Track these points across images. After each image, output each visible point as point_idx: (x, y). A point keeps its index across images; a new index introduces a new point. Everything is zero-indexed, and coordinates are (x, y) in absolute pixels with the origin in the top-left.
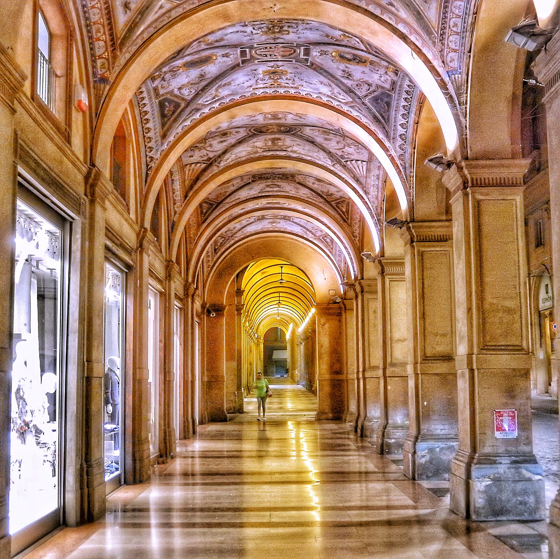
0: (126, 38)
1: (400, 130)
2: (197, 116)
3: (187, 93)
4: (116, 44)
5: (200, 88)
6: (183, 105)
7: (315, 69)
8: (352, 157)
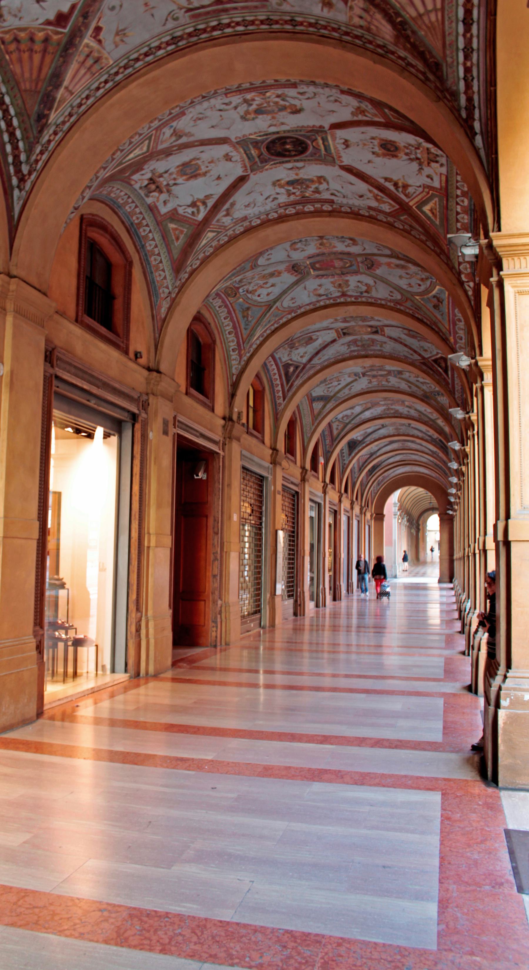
2: (364, 445)
3: (360, 438)
4: (333, 440)
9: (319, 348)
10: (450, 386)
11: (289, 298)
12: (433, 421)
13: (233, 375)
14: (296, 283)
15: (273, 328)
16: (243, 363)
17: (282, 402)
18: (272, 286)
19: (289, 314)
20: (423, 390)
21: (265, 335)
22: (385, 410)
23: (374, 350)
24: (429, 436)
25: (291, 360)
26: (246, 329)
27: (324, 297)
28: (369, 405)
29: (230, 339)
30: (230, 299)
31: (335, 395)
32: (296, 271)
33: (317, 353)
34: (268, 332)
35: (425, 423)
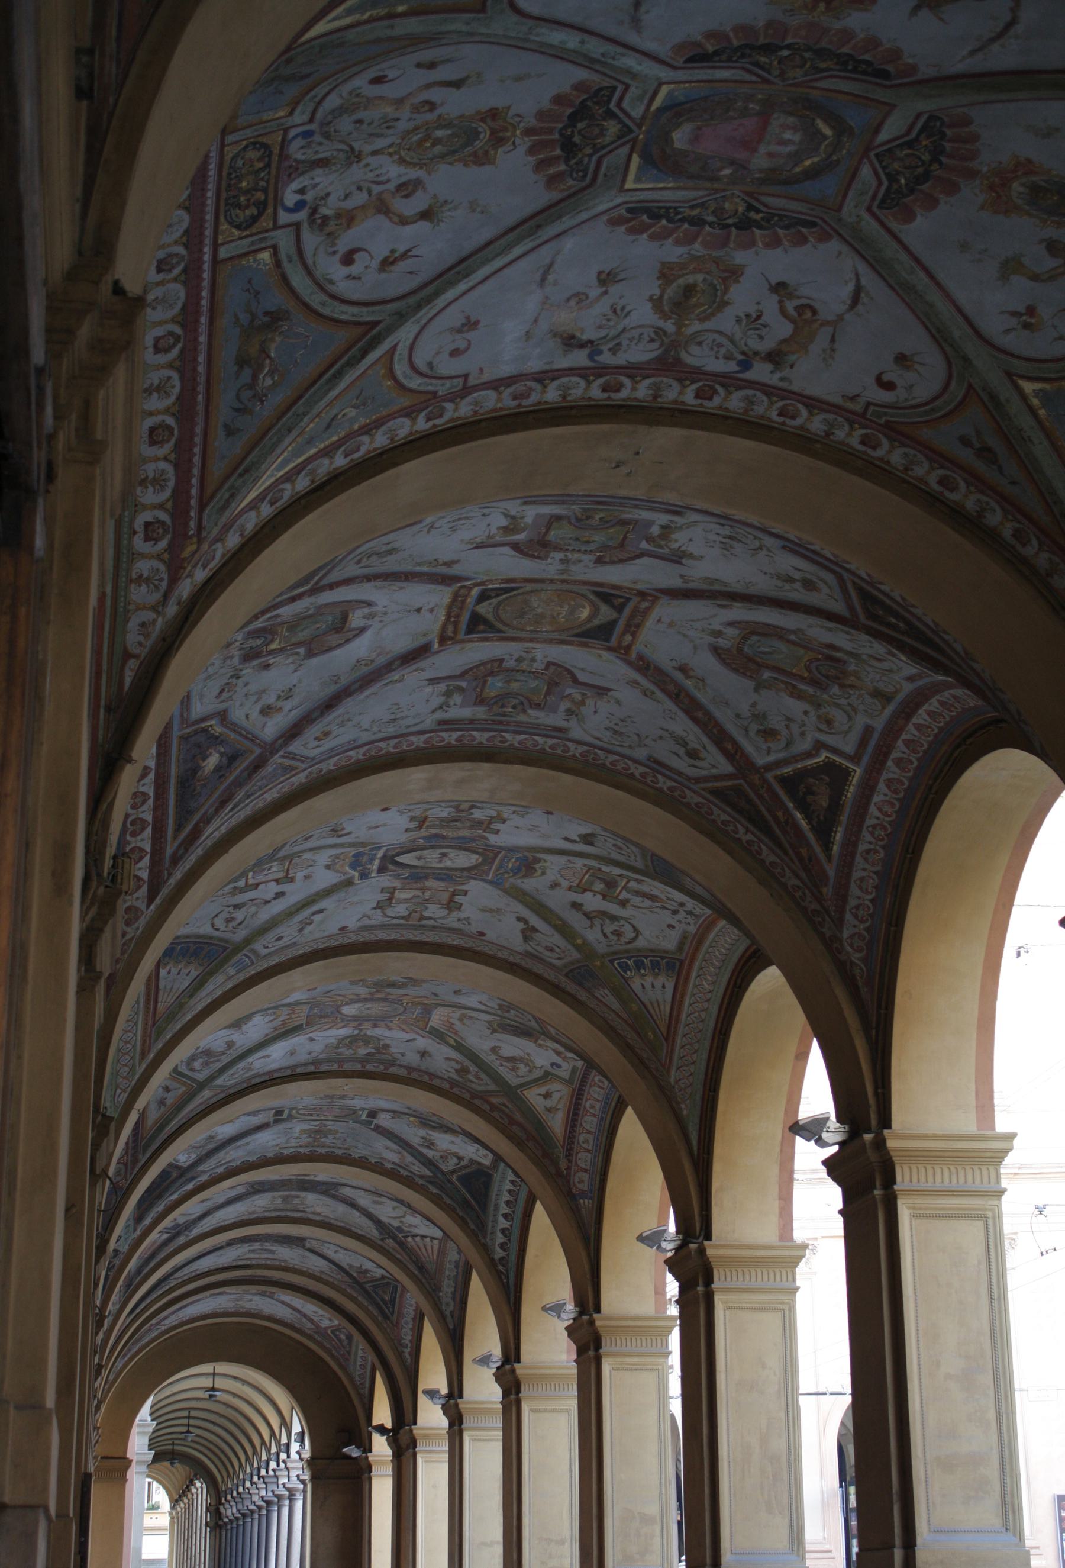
0: (153, 1138)
1: (503, 1223)
2: (190, 1186)
3: (184, 1160)
5: (204, 1152)
6: (174, 1175)
7: (379, 1133)
8: (416, 1231)
9: (344, 681)
10: (828, 891)
11: (453, 317)
12: (512, 1093)
13: (127, 655)
14: (531, 224)
15: (325, 467)
16: (172, 610)
17: (143, 907)
18: (426, 215)
19: (409, 413)
20: (585, 948)
21: (288, 492)
22: (341, 1041)
23: (536, 729)
24: (429, 1163)
25: (223, 716)
26: (230, 432)
27: (579, 358)
28: (301, 1016)
29: (150, 470)
30: (224, 227)
31: (248, 941)
32: (569, 148)
33: (330, 704)
34: (302, 484)
35: (470, 1101)
